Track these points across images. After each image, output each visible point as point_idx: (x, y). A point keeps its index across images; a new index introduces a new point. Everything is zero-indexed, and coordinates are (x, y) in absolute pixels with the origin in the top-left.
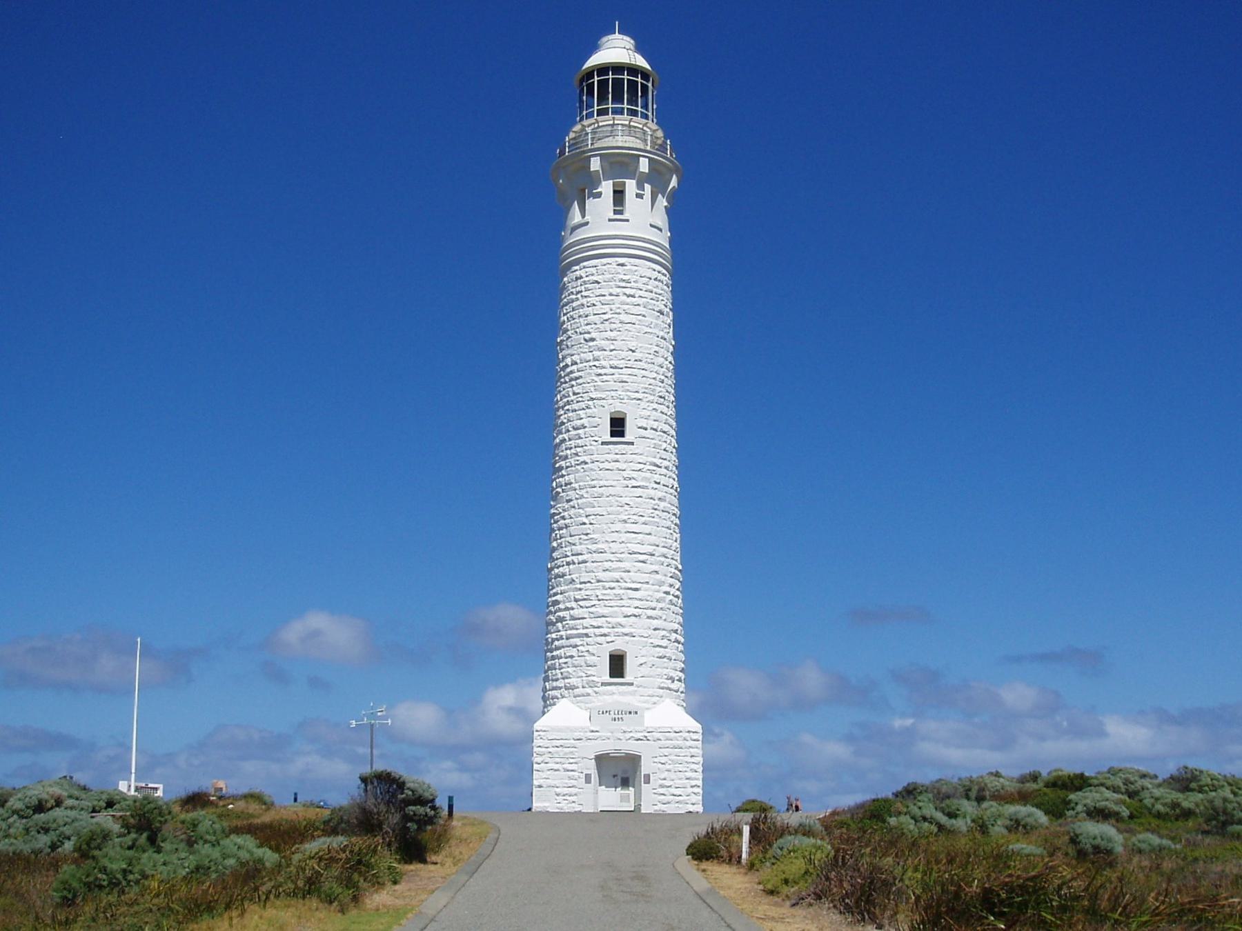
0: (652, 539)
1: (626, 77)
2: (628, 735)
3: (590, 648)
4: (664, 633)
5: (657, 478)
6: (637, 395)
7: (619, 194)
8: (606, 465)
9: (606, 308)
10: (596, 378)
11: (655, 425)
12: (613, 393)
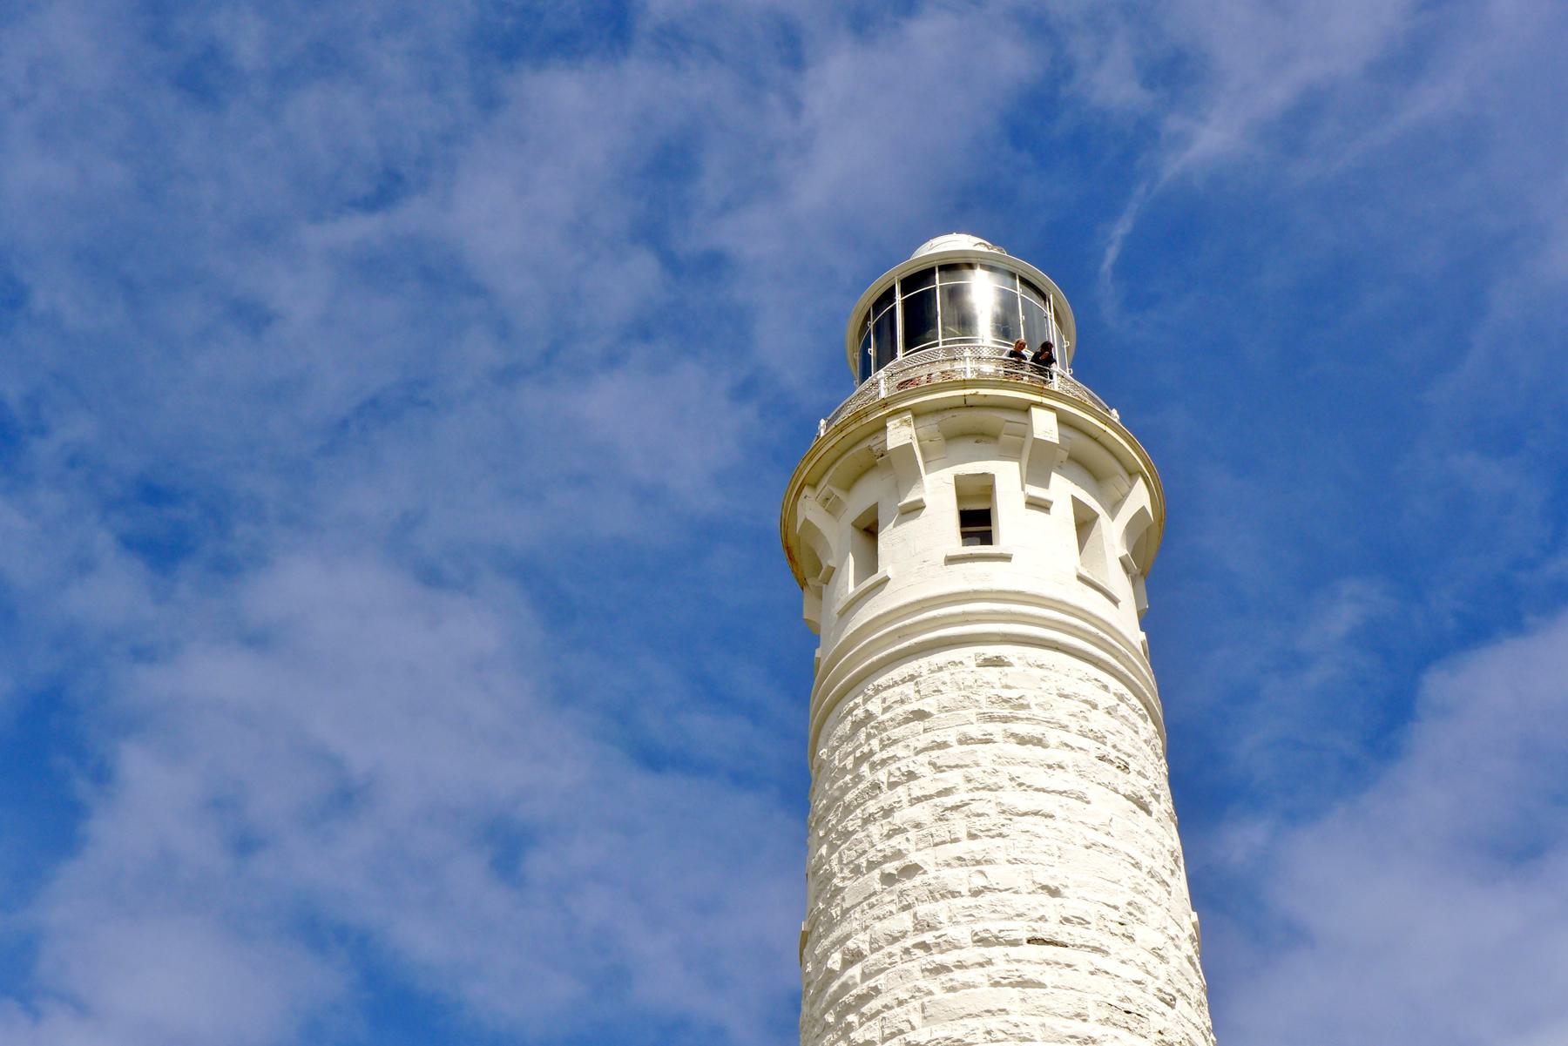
9: (953, 778)
10: (934, 984)
12: (994, 1023)
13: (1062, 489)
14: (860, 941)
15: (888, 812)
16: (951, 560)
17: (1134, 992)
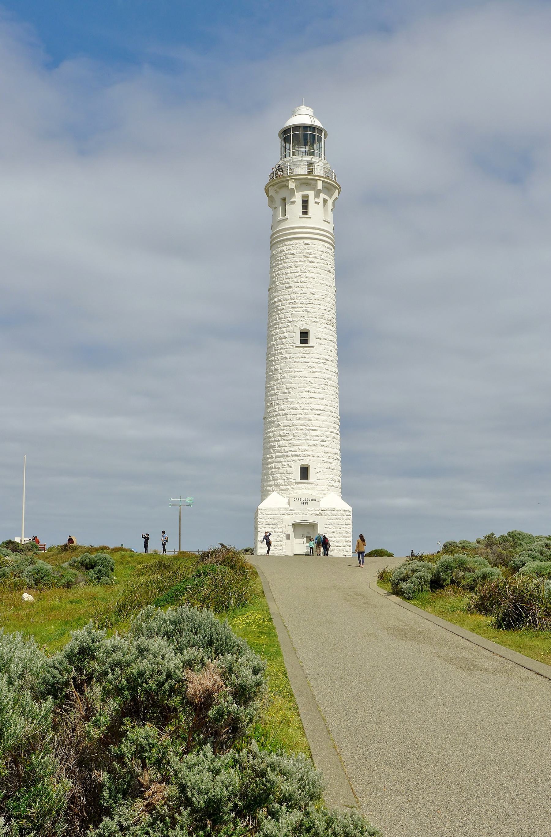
0: (324, 402)
1: (309, 132)
2: (311, 512)
3: (289, 463)
4: (330, 455)
5: (327, 367)
6: (315, 319)
7: (305, 202)
8: (298, 360)
10: (292, 310)
11: (326, 337)
12: (302, 319)
13: (322, 196)
14: (280, 298)
15: (287, 274)
16: (300, 217)
17: (324, 311)
